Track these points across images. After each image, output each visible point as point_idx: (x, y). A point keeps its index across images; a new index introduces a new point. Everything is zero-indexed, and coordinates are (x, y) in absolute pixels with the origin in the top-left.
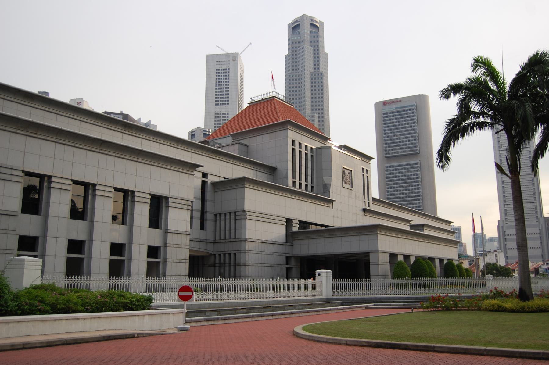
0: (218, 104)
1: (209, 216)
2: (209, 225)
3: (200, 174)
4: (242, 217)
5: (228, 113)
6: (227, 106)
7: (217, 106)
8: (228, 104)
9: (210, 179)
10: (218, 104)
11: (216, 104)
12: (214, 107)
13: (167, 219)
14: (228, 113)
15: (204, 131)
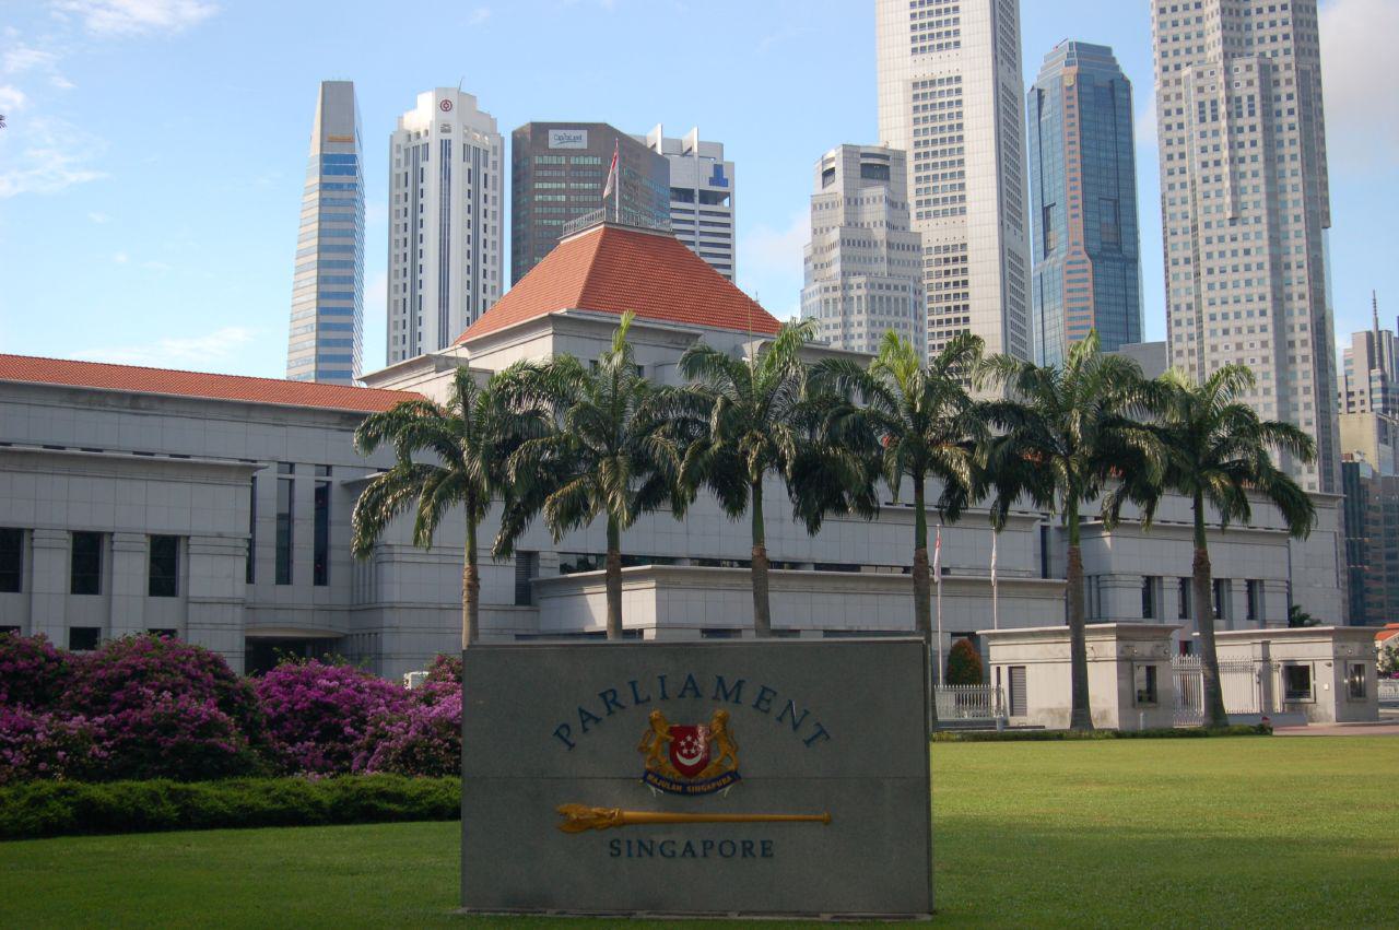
0: (923, 49)
1: (335, 556)
2: (336, 573)
3: (313, 470)
4: (385, 558)
5: (958, 79)
6: (952, 52)
7: (919, 57)
8: (957, 44)
9: (337, 478)
10: (923, 49)
11: (914, 51)
12: (909, 59)
13: (187, 577)
14: (958, 79)
15: (864, 155)
